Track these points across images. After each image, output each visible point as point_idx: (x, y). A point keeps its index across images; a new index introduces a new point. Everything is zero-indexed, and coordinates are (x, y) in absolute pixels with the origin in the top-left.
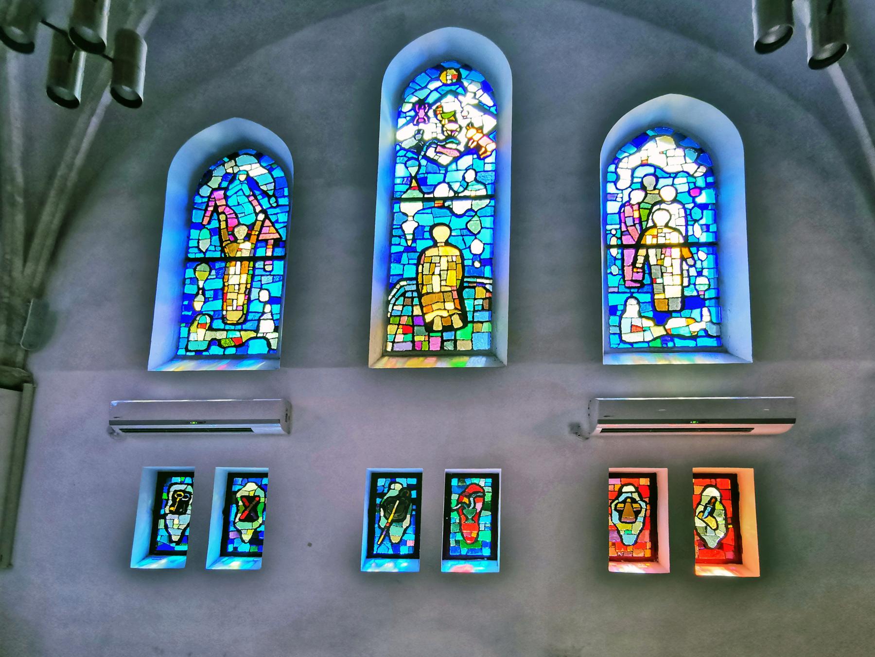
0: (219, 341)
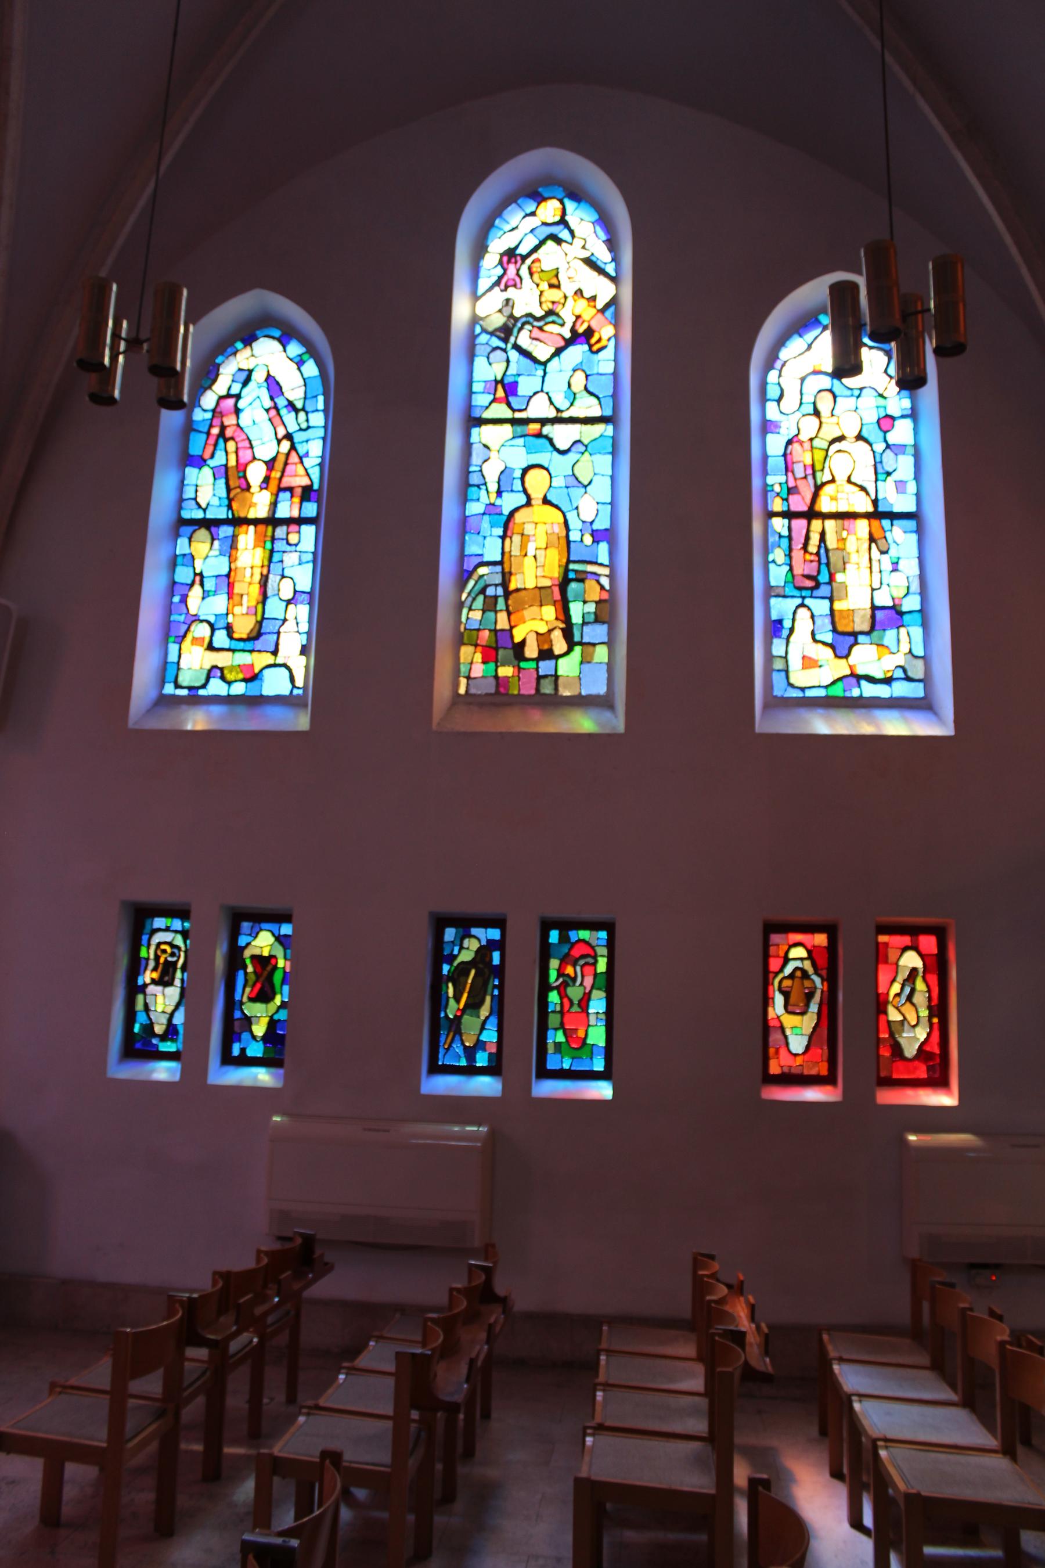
0: (222, 669)
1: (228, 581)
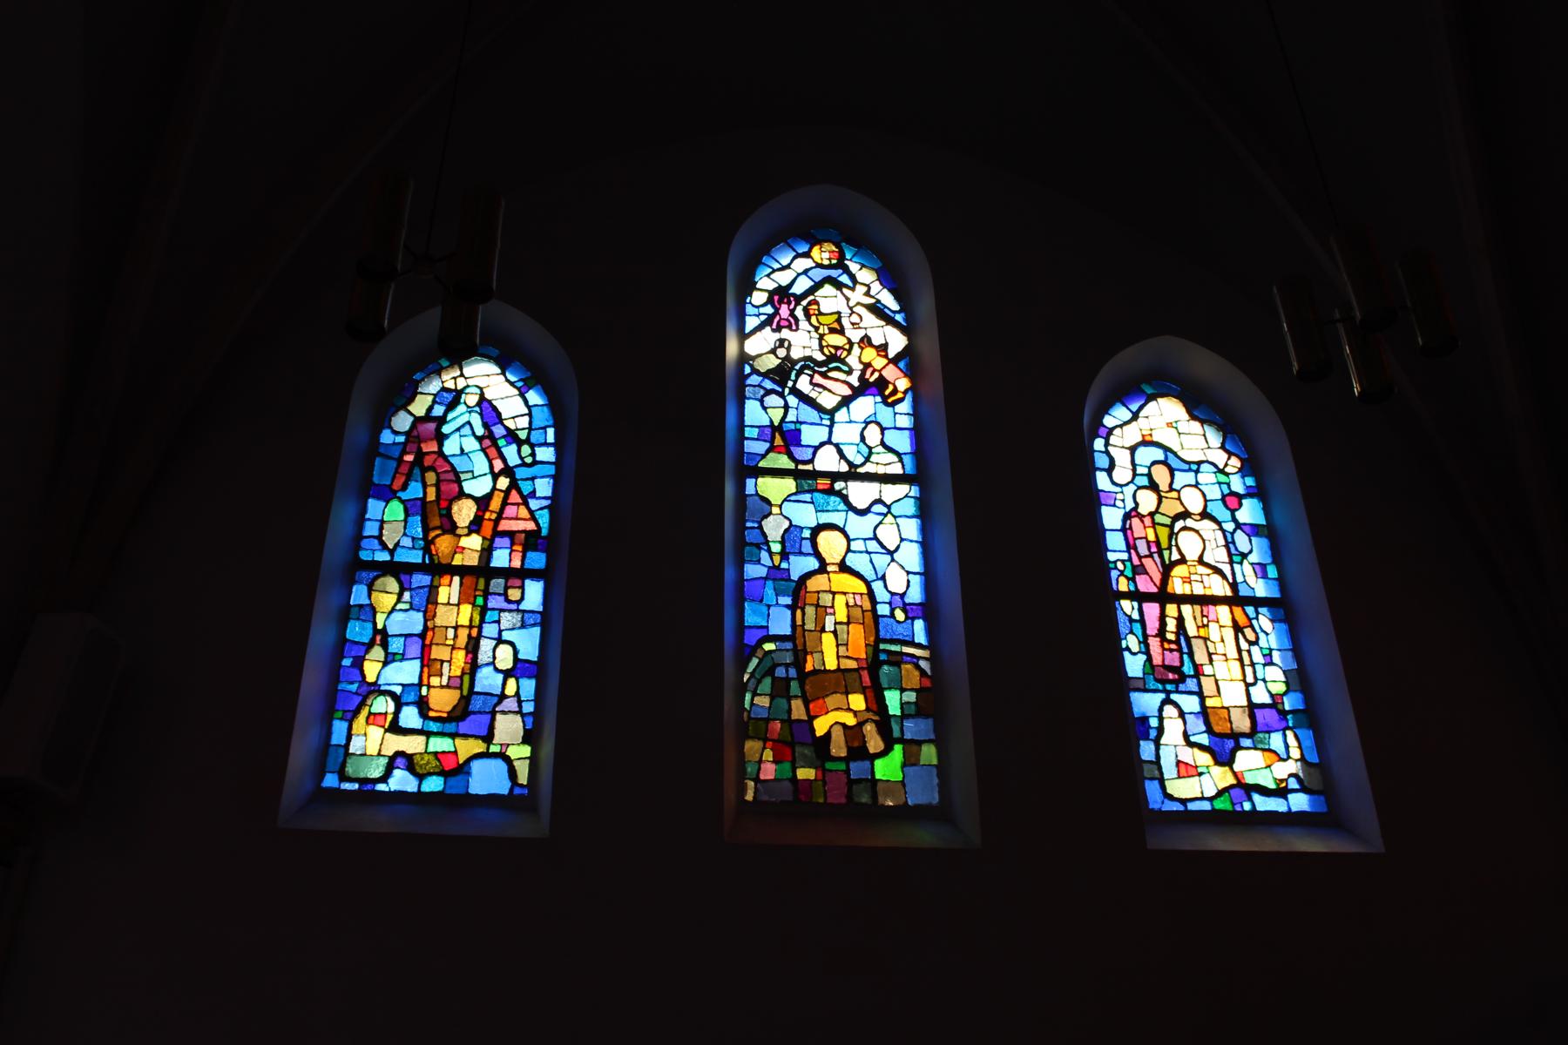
1: (424, 640)
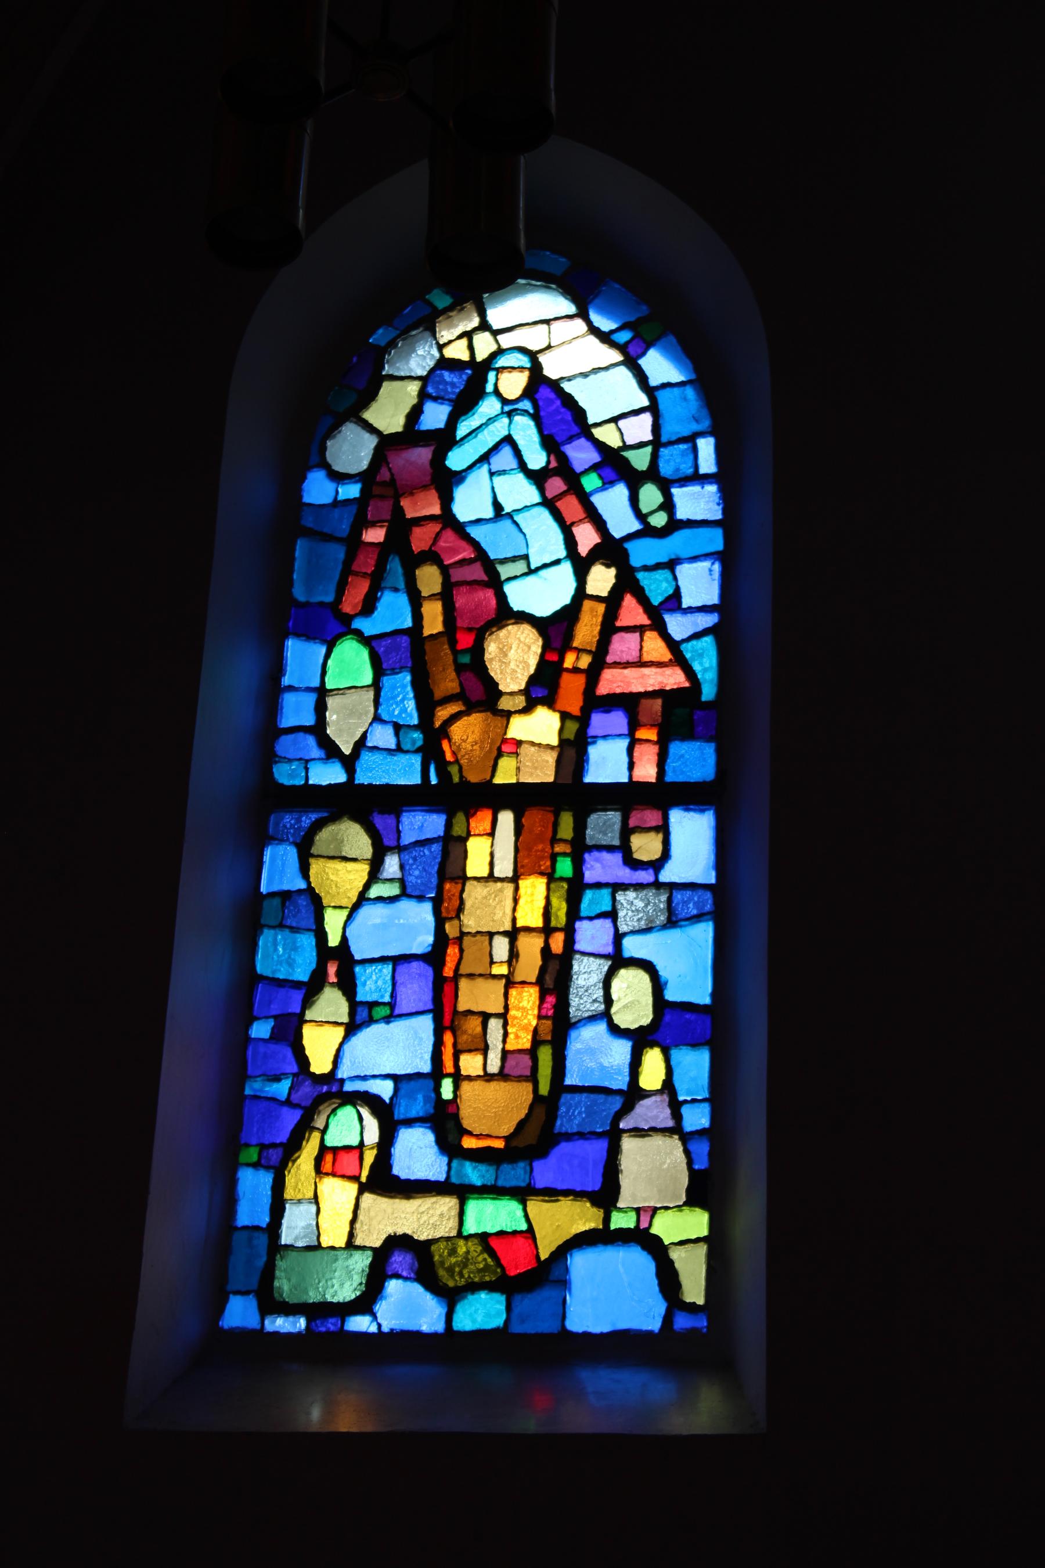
1: (440, 969)
